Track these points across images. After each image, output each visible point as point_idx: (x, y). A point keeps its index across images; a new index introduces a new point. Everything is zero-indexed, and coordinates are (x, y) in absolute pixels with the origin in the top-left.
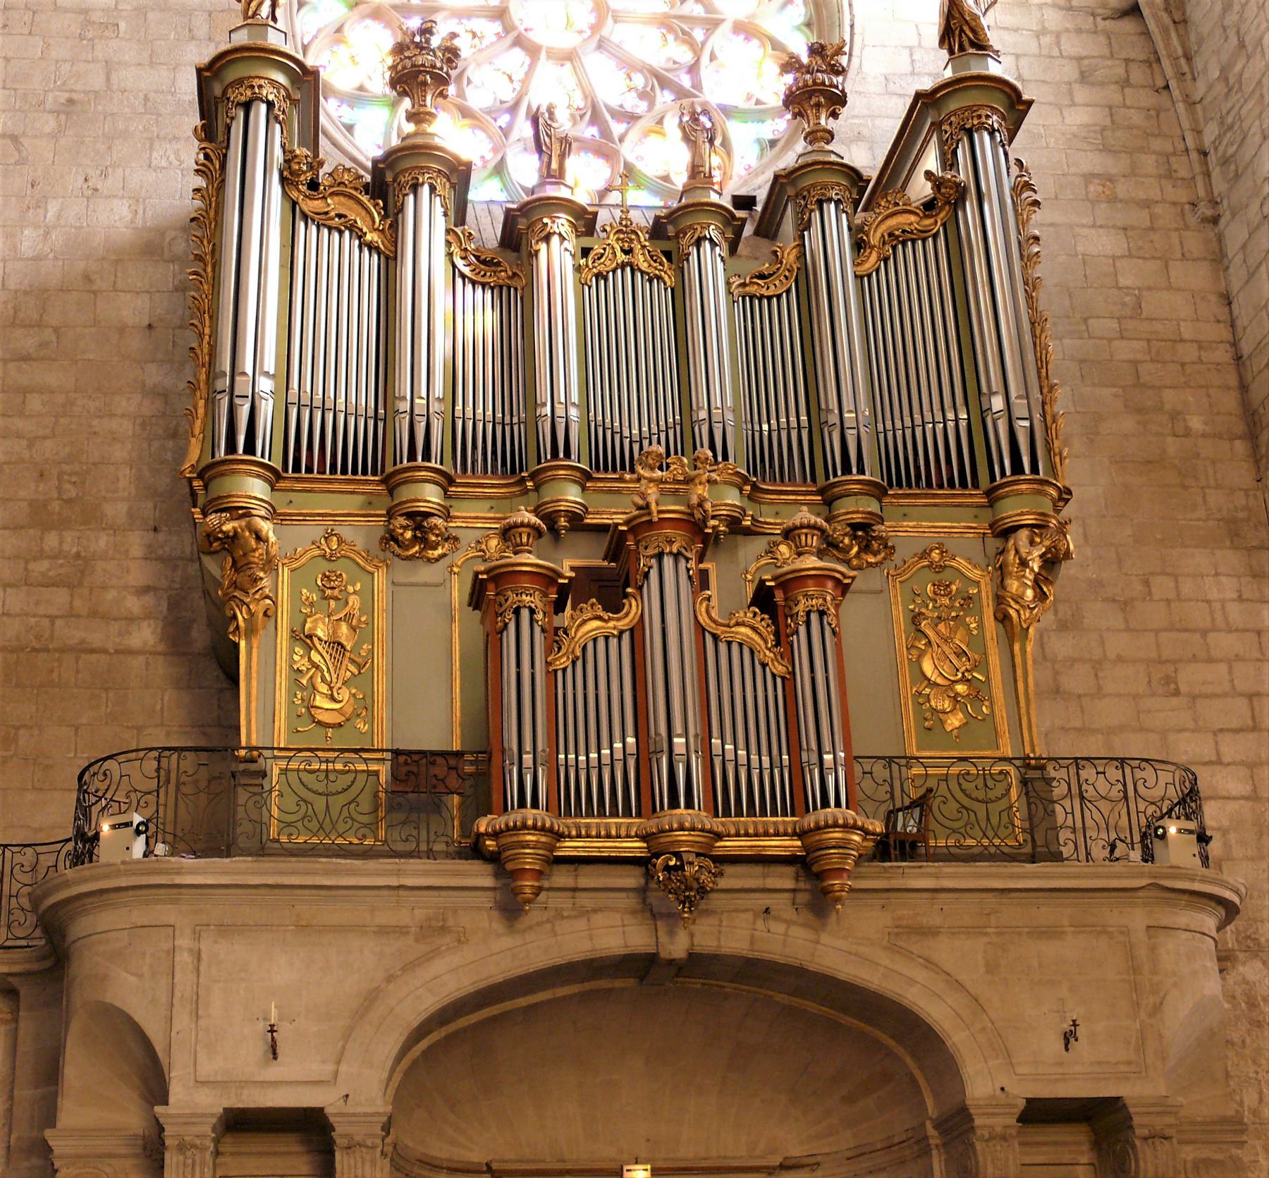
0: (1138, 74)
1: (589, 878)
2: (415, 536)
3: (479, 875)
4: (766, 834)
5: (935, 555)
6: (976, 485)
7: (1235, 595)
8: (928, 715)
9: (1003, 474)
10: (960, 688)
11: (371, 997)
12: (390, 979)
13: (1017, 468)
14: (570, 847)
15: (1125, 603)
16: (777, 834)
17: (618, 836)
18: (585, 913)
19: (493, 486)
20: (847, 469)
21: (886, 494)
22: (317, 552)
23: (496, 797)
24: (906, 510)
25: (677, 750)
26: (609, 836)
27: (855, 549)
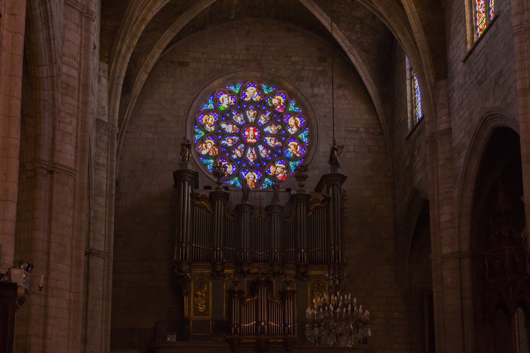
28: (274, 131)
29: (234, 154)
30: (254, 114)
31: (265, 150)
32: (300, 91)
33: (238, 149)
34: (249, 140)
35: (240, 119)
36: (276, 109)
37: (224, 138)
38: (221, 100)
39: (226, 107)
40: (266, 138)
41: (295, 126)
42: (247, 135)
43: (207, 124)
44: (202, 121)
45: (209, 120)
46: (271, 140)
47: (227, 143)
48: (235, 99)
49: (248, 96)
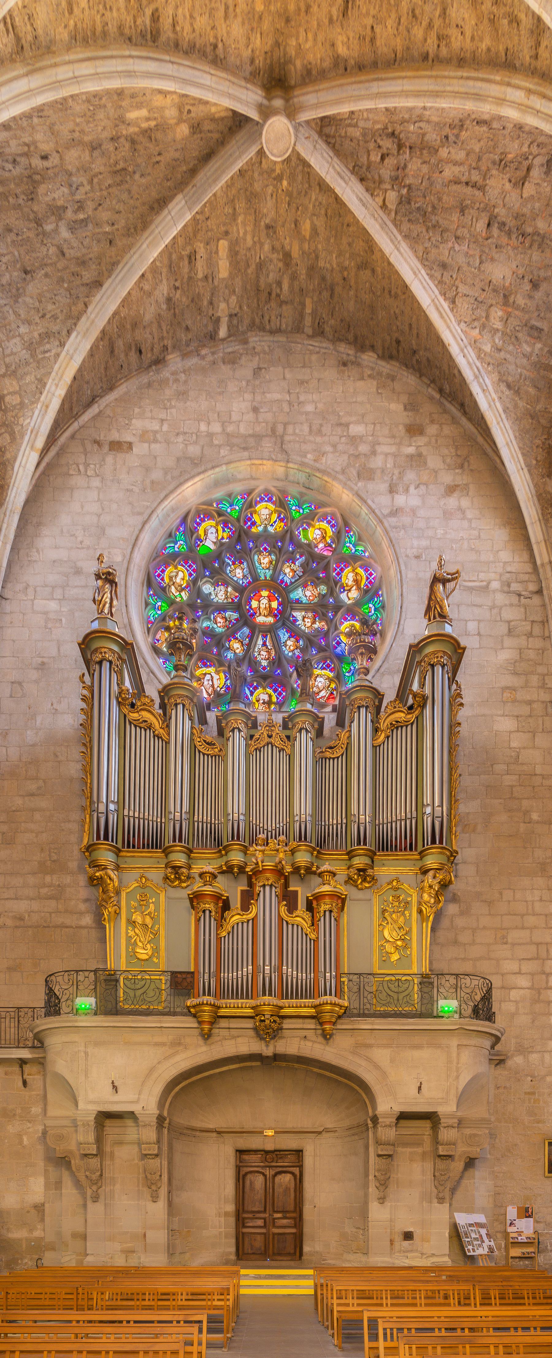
0: (537, 630)
1: (234, 1023)
2: (176, 877)
3: (190, 1022)
4: (301, 1007)
5: (394, 883)
6: (416, 850)
7: (539, 899)
8: (384, 955)
9: (427, 844)
10: (399, 943)
11: (152, 1070)
12: (159, 1063)
13: (433, 842)
14: (223, 1012)
15: (490, 902)
16: (305, 1007)
17: (242, 1007)
18: (234, 1037)
19: (209, 853)
20: (359, 844)
21: (375, 854)
22: (137, 885)
23: (196, 991)
24: (384, 862)
25: (266, 972)
26: (238, 1007)
27: (360, 881)
28: (311, 598)
29: (229, 649)
30: (271, 562)
31: (292, 639)
32: (365, 502)
33: (237, 639)
34: (260, 619)
35: (241, 574)
36: (316, 549)
37: (207, 614)
38: (201, 532)
39: (212, 547)
40: (295, 614)
41: (354, 588)
42: (256, 608)
43: (173, 587)
44: (163, 579)
45: (176, 576)
46: (304, 617)
47: (215, 626)
48: (231, 529)
49: (258, 522)
